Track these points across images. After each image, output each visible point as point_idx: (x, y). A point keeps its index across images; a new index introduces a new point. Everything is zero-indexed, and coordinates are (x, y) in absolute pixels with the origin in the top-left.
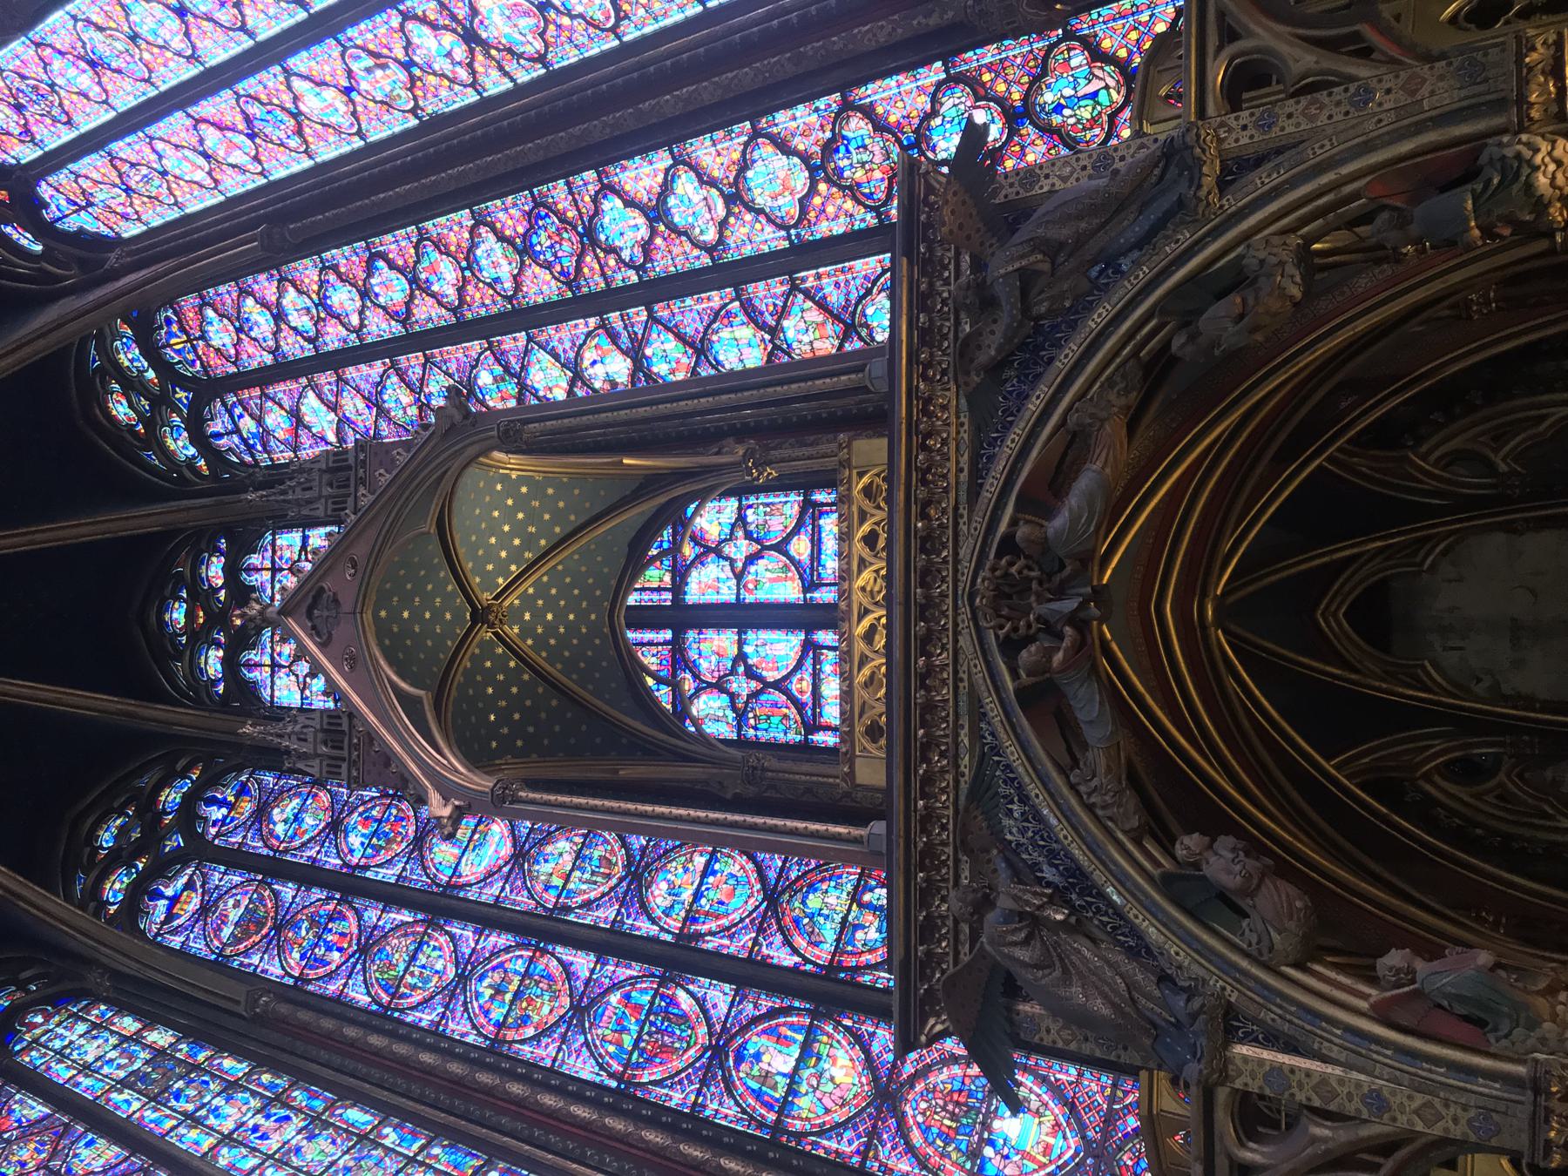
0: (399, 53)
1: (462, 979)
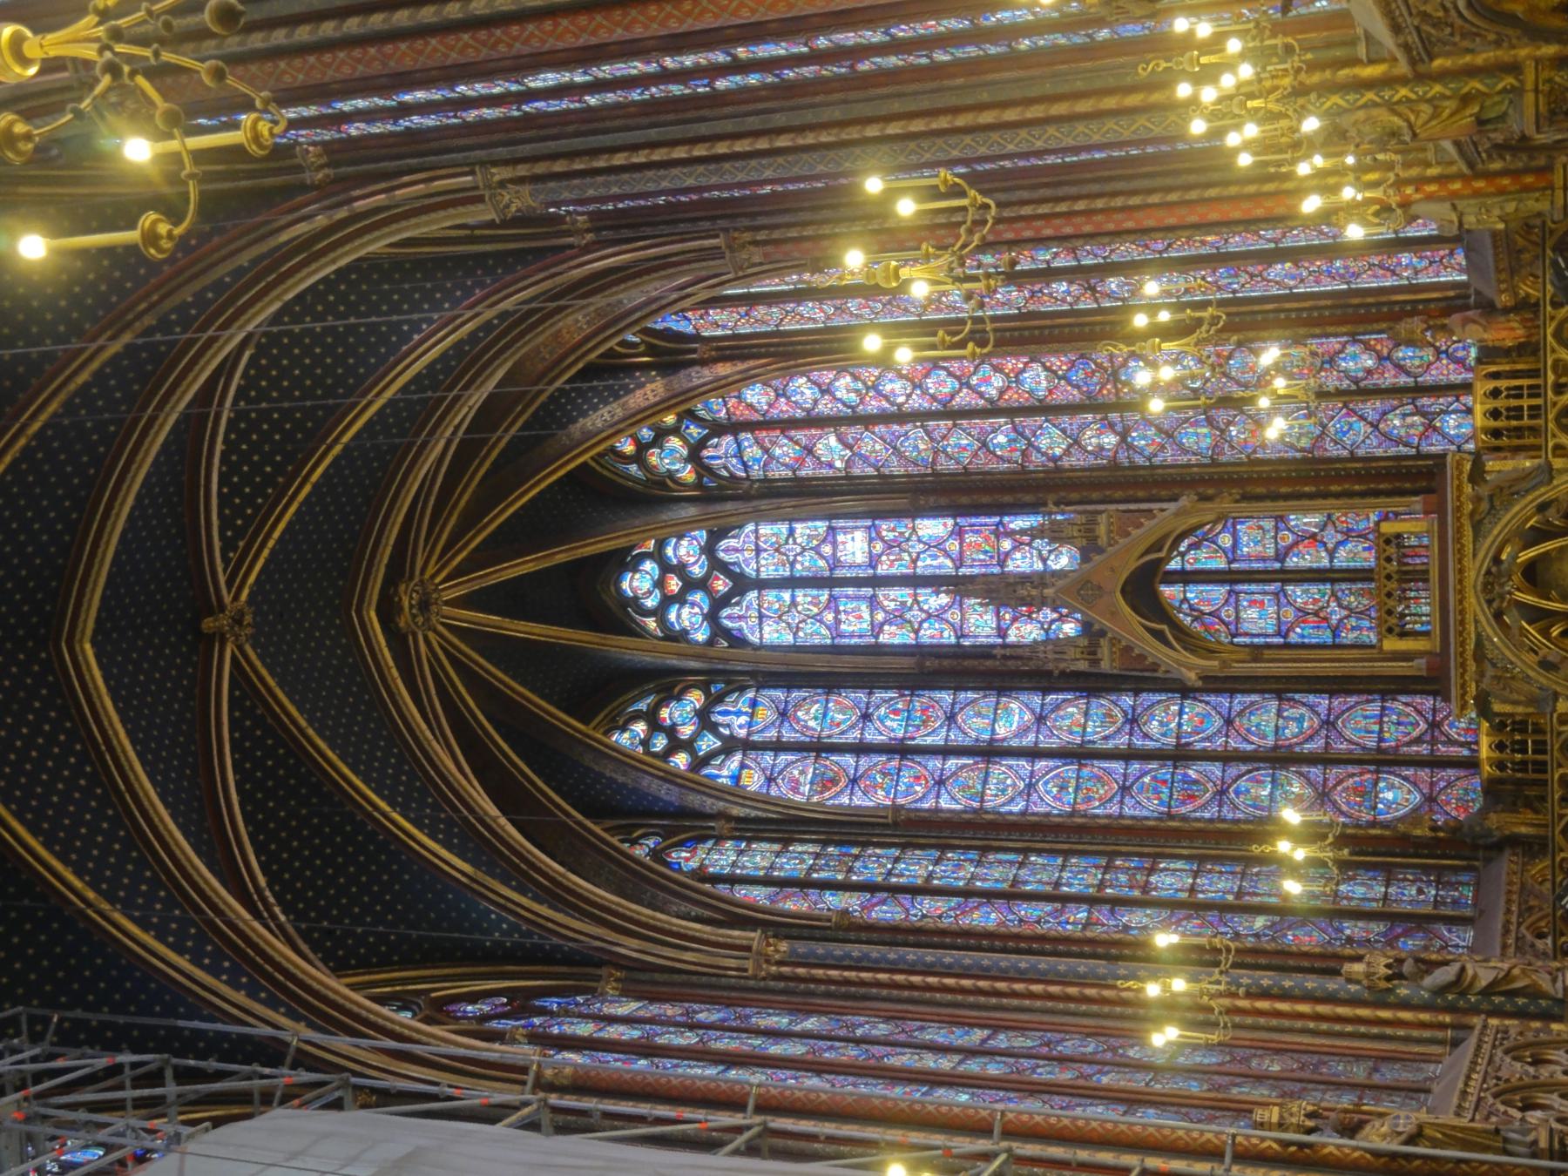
0: (1037, 288)
1: (1031, 787)
